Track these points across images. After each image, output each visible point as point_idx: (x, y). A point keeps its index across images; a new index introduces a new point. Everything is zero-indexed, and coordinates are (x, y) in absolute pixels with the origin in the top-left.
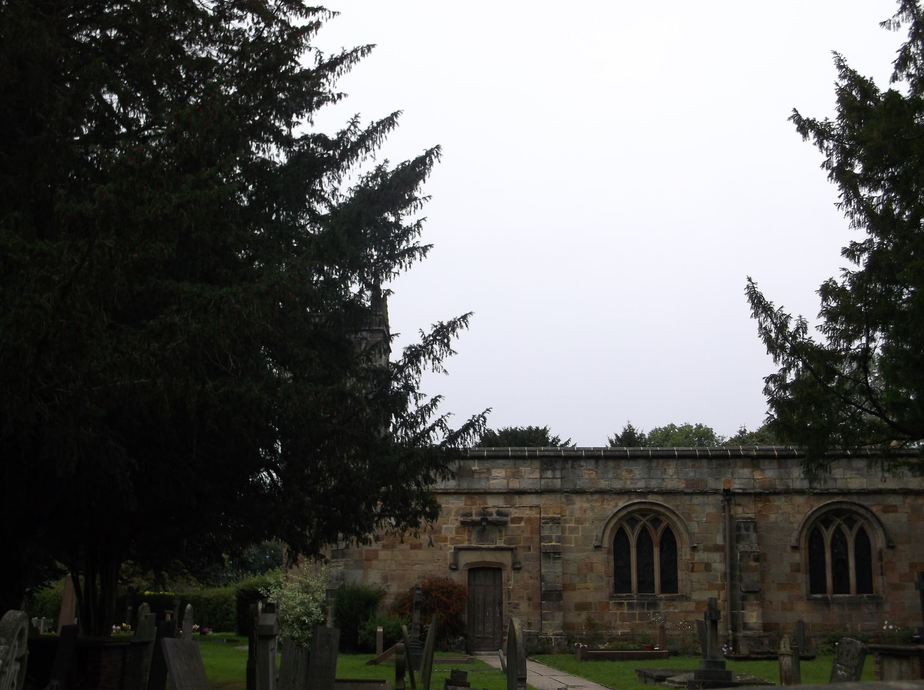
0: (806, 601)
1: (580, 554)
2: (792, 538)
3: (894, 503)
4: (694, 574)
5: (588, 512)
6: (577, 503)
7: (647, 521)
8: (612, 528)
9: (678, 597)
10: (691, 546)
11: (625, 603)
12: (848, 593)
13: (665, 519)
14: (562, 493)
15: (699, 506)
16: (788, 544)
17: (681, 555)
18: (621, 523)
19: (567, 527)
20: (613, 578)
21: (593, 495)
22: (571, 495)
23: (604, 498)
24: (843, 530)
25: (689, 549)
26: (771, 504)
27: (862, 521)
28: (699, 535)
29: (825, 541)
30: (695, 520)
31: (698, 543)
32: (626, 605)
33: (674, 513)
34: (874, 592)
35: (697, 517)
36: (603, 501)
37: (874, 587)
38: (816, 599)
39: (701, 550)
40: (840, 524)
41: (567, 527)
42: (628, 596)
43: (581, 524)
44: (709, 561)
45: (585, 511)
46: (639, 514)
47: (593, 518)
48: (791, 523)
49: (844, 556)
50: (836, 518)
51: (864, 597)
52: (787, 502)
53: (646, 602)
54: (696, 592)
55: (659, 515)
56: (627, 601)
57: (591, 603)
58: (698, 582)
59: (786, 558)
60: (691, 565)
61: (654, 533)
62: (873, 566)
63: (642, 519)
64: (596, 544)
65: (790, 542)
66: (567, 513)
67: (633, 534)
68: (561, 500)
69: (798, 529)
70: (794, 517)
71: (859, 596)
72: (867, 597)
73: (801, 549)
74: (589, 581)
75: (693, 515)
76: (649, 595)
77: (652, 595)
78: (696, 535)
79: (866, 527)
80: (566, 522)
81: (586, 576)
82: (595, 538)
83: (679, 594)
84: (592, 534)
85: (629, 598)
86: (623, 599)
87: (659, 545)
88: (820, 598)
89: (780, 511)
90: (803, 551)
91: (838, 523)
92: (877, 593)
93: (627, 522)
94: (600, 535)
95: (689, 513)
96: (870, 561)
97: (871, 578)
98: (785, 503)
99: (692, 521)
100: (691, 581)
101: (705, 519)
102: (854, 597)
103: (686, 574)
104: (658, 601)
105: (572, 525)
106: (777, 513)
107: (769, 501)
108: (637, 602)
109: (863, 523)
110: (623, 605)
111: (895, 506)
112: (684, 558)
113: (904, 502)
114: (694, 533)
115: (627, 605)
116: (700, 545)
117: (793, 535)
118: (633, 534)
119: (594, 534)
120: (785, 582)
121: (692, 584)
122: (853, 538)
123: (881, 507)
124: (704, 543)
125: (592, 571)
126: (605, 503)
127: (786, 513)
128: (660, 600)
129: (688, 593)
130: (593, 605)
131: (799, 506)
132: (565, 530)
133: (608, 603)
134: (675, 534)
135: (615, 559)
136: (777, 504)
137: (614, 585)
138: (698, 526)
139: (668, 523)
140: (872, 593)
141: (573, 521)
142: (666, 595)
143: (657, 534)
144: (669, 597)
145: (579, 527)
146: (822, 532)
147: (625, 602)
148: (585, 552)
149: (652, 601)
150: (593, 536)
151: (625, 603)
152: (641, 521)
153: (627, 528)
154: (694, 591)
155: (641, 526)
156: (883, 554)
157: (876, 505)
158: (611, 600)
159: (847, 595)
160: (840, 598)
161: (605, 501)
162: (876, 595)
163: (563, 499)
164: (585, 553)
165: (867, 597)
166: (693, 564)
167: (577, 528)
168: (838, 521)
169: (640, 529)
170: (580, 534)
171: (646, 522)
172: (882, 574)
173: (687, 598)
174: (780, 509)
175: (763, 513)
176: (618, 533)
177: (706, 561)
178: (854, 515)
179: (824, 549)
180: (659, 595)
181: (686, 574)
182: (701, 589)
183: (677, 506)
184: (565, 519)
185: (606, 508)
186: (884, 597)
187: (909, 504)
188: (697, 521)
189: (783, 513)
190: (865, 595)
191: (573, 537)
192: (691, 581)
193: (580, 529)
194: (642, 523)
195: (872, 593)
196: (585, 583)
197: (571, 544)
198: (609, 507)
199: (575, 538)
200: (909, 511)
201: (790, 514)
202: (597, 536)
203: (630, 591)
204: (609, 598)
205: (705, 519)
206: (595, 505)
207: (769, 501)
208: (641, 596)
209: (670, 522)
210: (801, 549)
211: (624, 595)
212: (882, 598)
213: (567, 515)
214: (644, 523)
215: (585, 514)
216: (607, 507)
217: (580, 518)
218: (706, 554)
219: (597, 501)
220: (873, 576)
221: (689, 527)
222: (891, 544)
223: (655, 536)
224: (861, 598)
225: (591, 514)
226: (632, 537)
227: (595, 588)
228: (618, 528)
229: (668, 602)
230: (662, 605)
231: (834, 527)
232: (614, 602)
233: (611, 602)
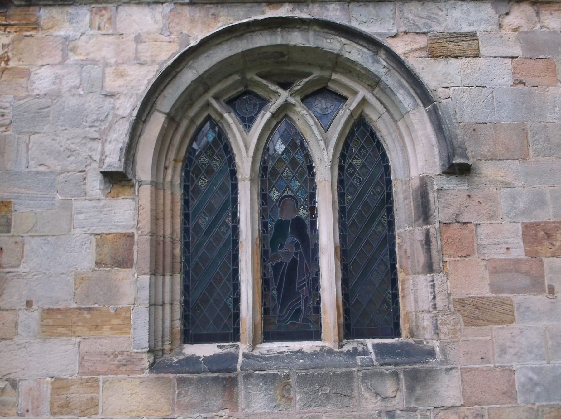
0: (147, 374)
2: (109, 148)
3: (465, 29)
12: (316, 335)
16: (95, 165)
24: (300, 124)
26: (39, 34)
27: (363, 92)
29: (237, 160)
34: (404, 332)
37: (402, 313)
38: (193, 361)
40: (286, 106)
48: (112, 95)
49: (302, 213)
50: (274, 88)
51: (365, 353)
52: (99, 29)
59: (81, 217)
62: (397, 241)
65: (102, 161)
69: (131, 115)
70: (121, 75)
71: (350, 345)
72: (377, 347)
73: (141, 183)
79: (371, 115)
88: (208, 360)
89: (73, 58)
90: (146, 192)
91: (275, 105)
92: (412, 335)
96: (391, 224)
97: (394, 282)
98: (95, 32)
102: (330, 352)
106: (62, 63)
107: (36, 26)
109: (364, 101)
111: (472, 36)
113: (500, 26)
117: (113, 136)
120: (74, 306)
122: (331, 149)
123: (422, 41)
127: (94, 62)
131: (138, 39)
136: (62, 33)
140: (397, 334)
146: (230, 136)
156: (432, 196)
157: (406, 33)
159: (307, 346)
160: (279, 357)
162: (411, 341)
165: (377, 347)
168: (284, 95)
172: (430, 268)
174: (73, 50)
175: (11, 64)
178: (334, 76)
179: (235, 187)
186: (437, 346)
187: (515, 30)
189: (81, 65)
190: (370, 342)
195: (397, 334)
200: (517, 51)
201: (107, 65)
207: (36, 26)
210: (141, 183)
212: (431, 353)
220: (401, 276)
222: (458, 160)
224: (355, 352)
231: (268, 115)
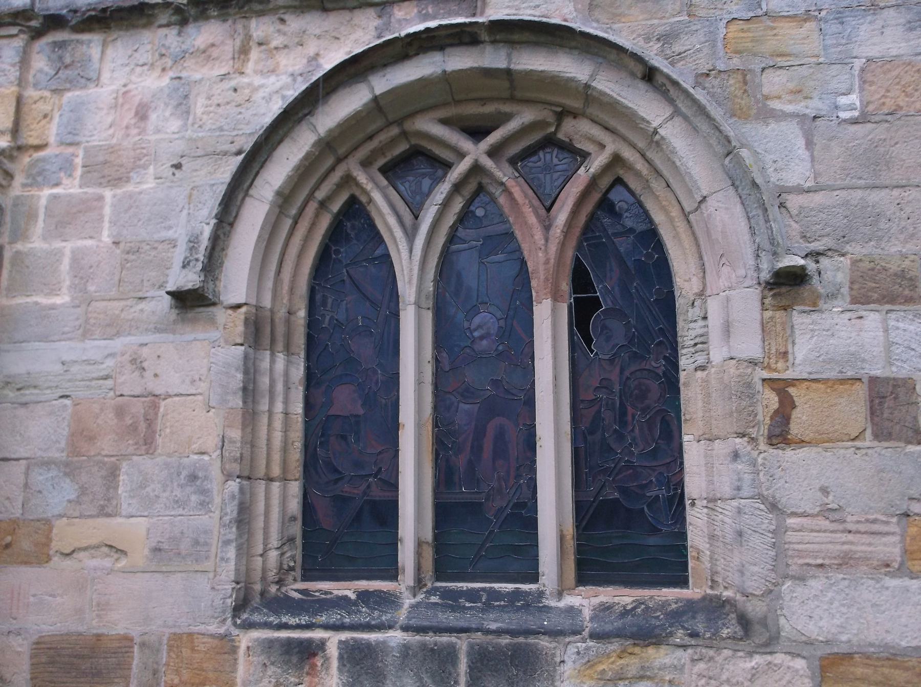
1: (95, 348)
4: (789, 455)
5: (153, 117)
6: (105, 76)
7: (492, 153)
8: (284, 198)
9: (690, 608)
10: (765, 275)
11: (333, 650)
13: (596, 132)
14: (37, 34)
15: (811, 25)
17: (702, 342)
18: (348, 180)
19: (43, 202)
20: (295, 488)
21: (191, 29)
22: (85, 37)
23: (248, 37)
25: (755, 293)
28: (818, 198)
30: (789, 108)
31: (815, 255)
32: (335, 664)
33: (650, 75)
35: (798, 93)
36: (244, 51)
39: (832, 296)
41: (43, 202)
42: (364, 596)
43: (117, 181)
44: (900, 370)
45: (142, 114)
46: (445, 122)
47: (180, 146)
53: (462, 644)
54: (815, 585)
55: (562, 114)
56: (345, 636)
57: (128, 639)
58: (826, 512)
60: (772, 400)
61: (532, 219)
63: (466, 144)
64: (190, 279)
66: (52, 132)
67: (411, 236)
68: (24, 62)
74: (125, 508)
75: (773, 82)
76: (494, 595)
77: (517, 593)
78: (793, 202)
80: (38, 177)
81: (113, 474)
82: (180, 253)
83: (693, 592)
84: (170, 234)
85: (364, 615)
86: (323, 619)
87: (565, 286)
93: (384, 170)
94: (207, 231)
95: (744, 74)
99: (767, 115)
100: (774, 507)
101: (854, 98)
103: (736, 456)
104: (544, 642)
105: (71, 187)
108: (405, 649)
110: (319, 661)
112: (717, 353)
114: (782, 191)
115: (341, 658)
116: (825, 262)
118: (411, 236)
119: (180, 234)
121: (778, 531)
124: (856, 250)
125: (148, 443)
126: (250, 66)
128: (554, 634)
129: (754, 585)
130: (137, 658)
132: (32, 216)
133: (227, 645)
134: (658, 217)
135: (311, 380)
137: (296, 529)
138: (809, 144)
139: (617, 160)
141: (79, 172)
142: (607, 595)
143: (547, 228)
144: (625, 613)
145: (101, 198)
147: (334, 641)
148: (118, 334)
149: (505, 640)
150: (173, 243)
151: (333, 650)
152: (462, 155)
153: (377, 196)
154: (801, 579)
155: (457, 188)
158: (249, 626)
161: (255, 54)
163: (40, 63)
164: (118, 344)
166: (781, 387)
167: (91, 206)
169: (458, 205)
170: (106, 237)
171: (488, 163)
173: (745, 622)
176: (336, 234)
177: (878, 372)
180: (560, 595)
181: (736, 456)
182: (846, 561)
183: (666, 38)
184: (43, 160)
185: (256, 89)
188: (800, 117)
191: (68, 252)
192: (774, 507)
193: (107, 211)
194: (462, 167)
196: (104, 513)
197: (54, 291)
198: (273, 79)
199: (76, 260)
202: (193, 242)
203: (393, 574)
204: (238, 609)
205: (854, 98)
206: (197, 76)
208: (447, 594)
209: (628, 154)
211: (347, 589)
213: (52, 139)
214: (476, 169)
215: (143, 131)
216: (258, 81)
217: (112, 150)
218: (872, 319)
219: (206, 54)
221: (744, 153)
223: (538, 235)
225: (174, 125)
226: (403, 245)
227: (157, 550)
228: (336, 207)
229: (614, 646)
230: (568, 669)
232: (270, 644)
233: (246, 639)
